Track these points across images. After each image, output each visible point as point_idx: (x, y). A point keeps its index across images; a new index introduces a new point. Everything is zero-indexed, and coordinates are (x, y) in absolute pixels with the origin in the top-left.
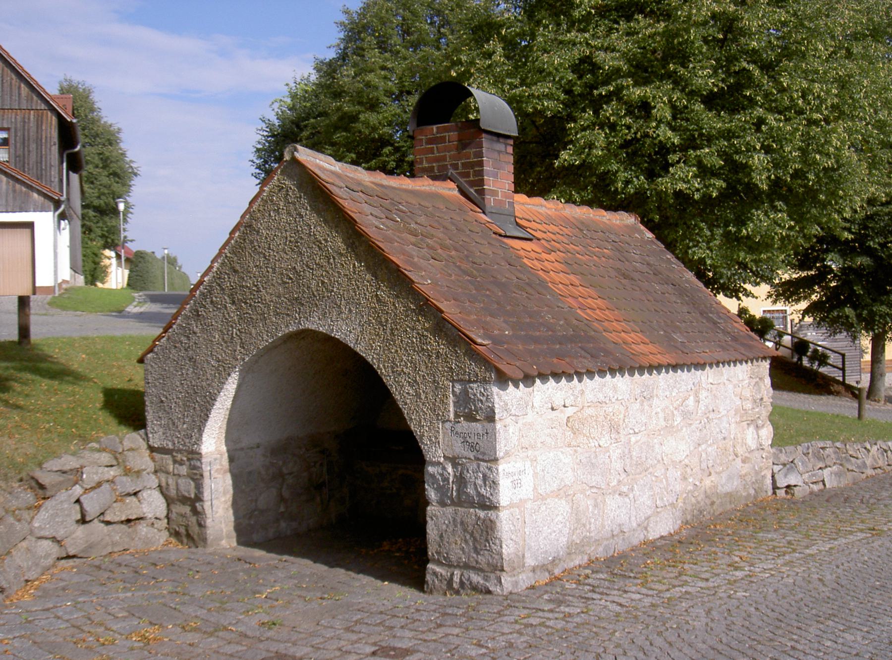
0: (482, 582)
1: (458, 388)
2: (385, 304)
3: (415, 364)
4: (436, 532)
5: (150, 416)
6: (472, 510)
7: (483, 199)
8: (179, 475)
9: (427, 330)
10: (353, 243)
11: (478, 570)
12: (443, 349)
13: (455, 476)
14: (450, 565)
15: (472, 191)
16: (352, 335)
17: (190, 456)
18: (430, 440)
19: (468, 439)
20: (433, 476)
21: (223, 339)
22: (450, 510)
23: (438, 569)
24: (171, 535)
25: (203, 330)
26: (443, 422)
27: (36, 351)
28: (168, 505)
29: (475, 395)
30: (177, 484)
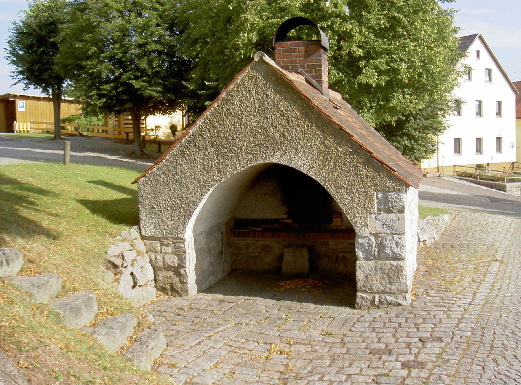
0: (394, 300)
1: (380, 195)
2: (330, 148)
3: (351, 182)
4: (362, 275)
5: (143, 217)
6: (387, 261)
7: (322, 86)
8: (166, 253)
9: (360, 163)
10: (307, 112)
11: (390, 293)
12: (370, 174)
13: (377, 243)
14: (372, 292)
15: (314, 81)
16: (305, 166)
17: (175, 241)
18: (361, 224)
19: (386, 223)
20: (362, 244)
21: (204, 168)
22: (372, 263)
23: (364, 295)
24: (158, 290)
25: (187, 163)
26: (370, 214)
27: (4, 177)
28: (155, 272)
29: (392, 199)
30: (164, 258)
